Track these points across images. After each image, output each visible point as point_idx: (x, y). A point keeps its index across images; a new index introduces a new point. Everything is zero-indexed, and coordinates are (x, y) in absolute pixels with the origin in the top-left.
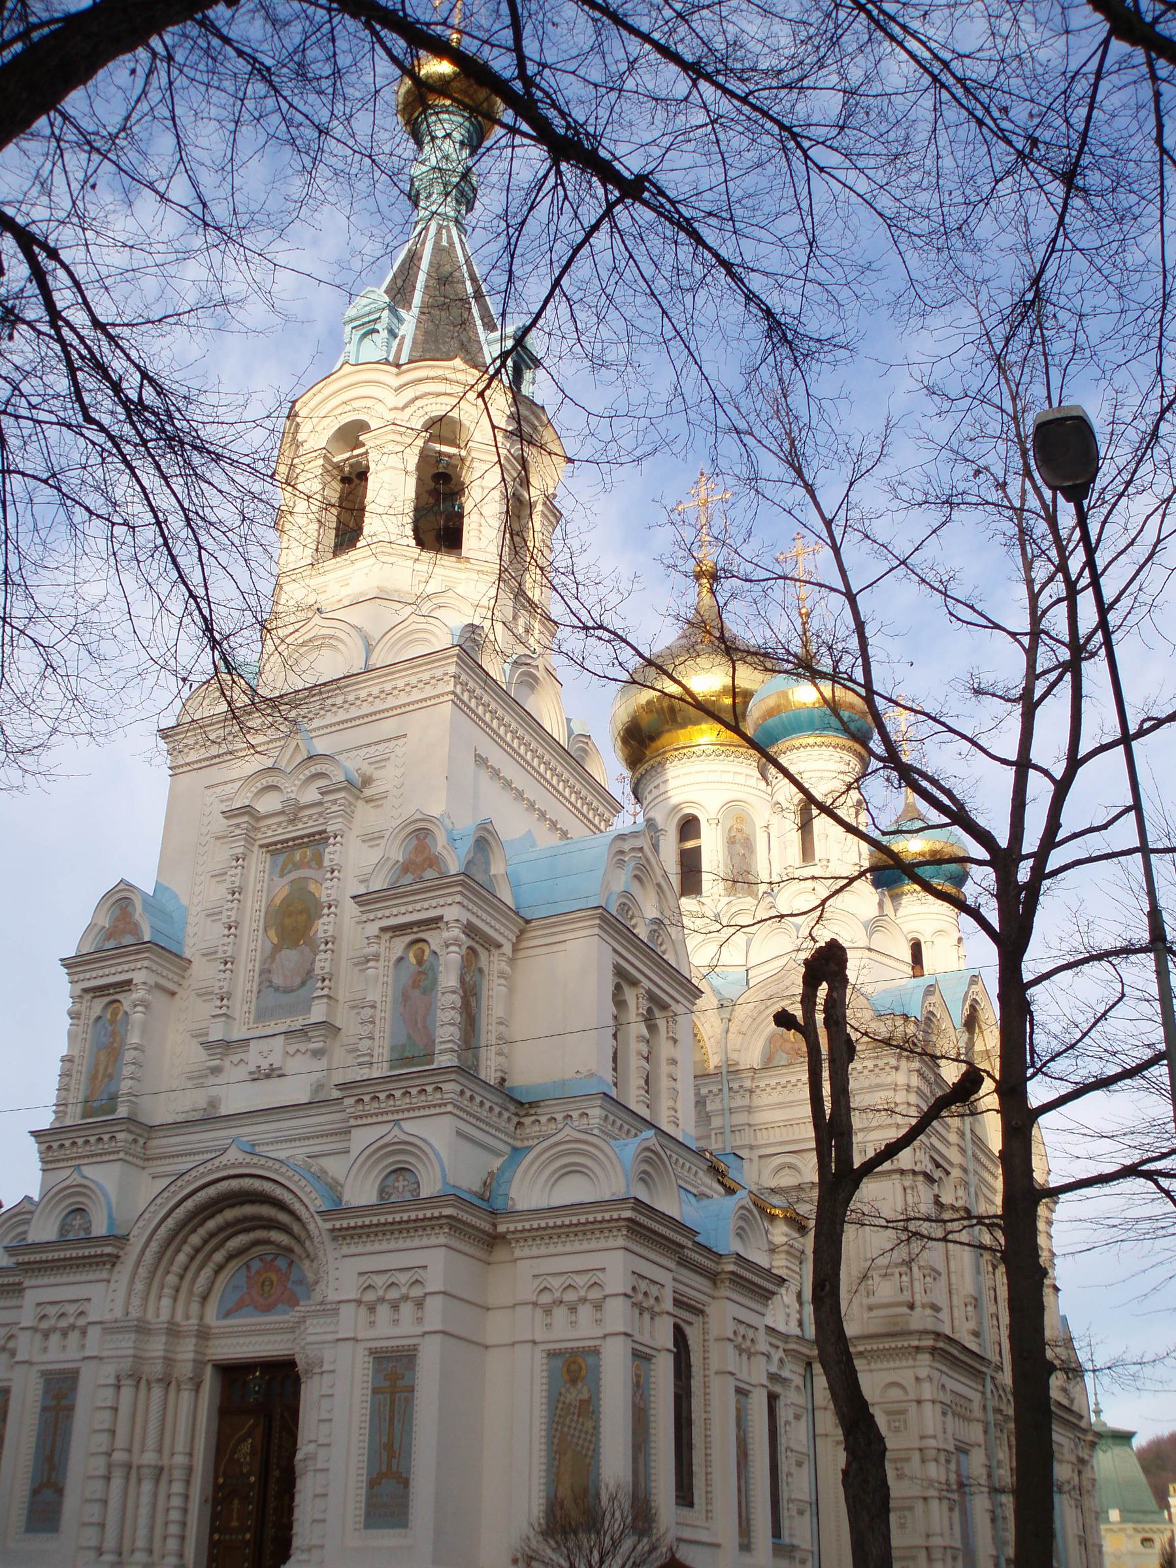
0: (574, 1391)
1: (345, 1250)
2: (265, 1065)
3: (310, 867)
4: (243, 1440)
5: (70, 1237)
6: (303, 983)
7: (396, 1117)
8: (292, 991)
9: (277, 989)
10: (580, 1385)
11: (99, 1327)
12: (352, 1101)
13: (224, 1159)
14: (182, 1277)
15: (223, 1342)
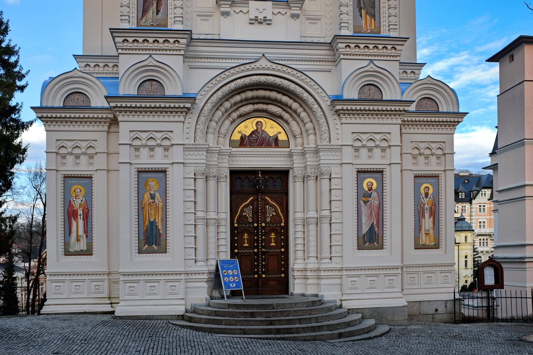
11: (182, 146)
15: (238, 159)
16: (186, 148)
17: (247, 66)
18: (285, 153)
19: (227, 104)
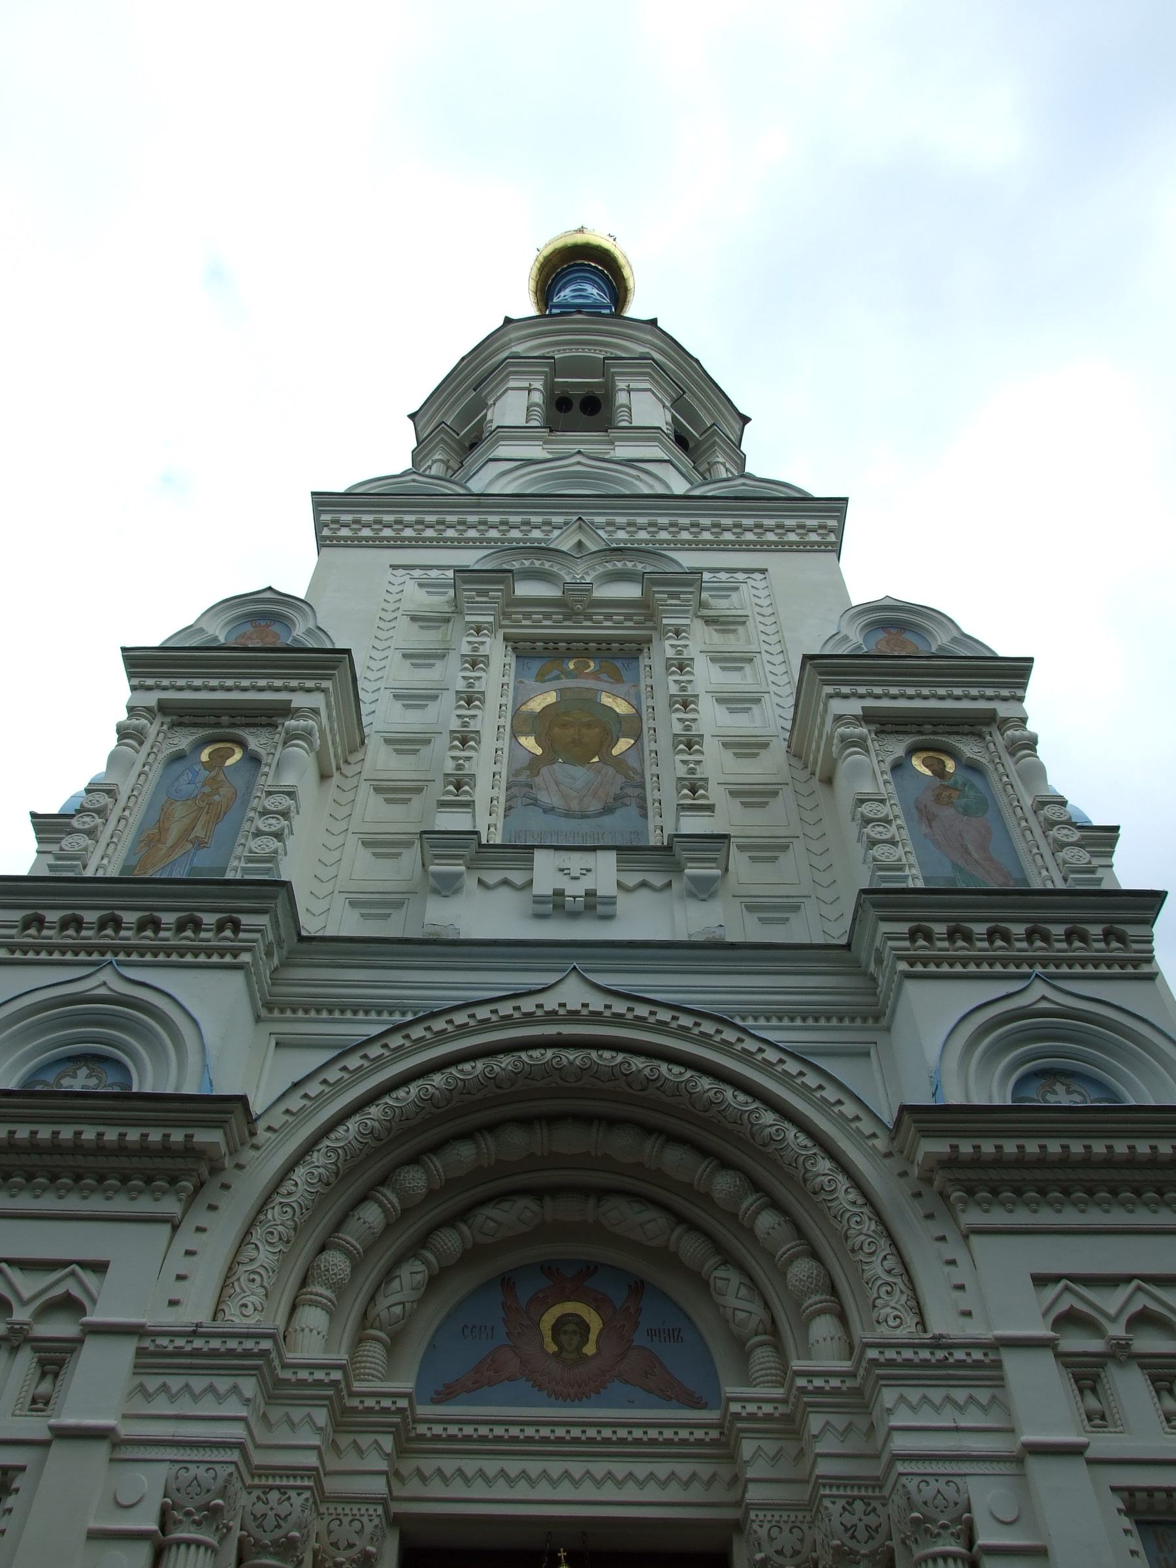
1: (973, 1217)
2: (575, 889)
3: (599, 679)
8: (584, 816)
11: (126, 1349)
12: (904, 928)
13: (550, 1002)
18: (699, 1434)
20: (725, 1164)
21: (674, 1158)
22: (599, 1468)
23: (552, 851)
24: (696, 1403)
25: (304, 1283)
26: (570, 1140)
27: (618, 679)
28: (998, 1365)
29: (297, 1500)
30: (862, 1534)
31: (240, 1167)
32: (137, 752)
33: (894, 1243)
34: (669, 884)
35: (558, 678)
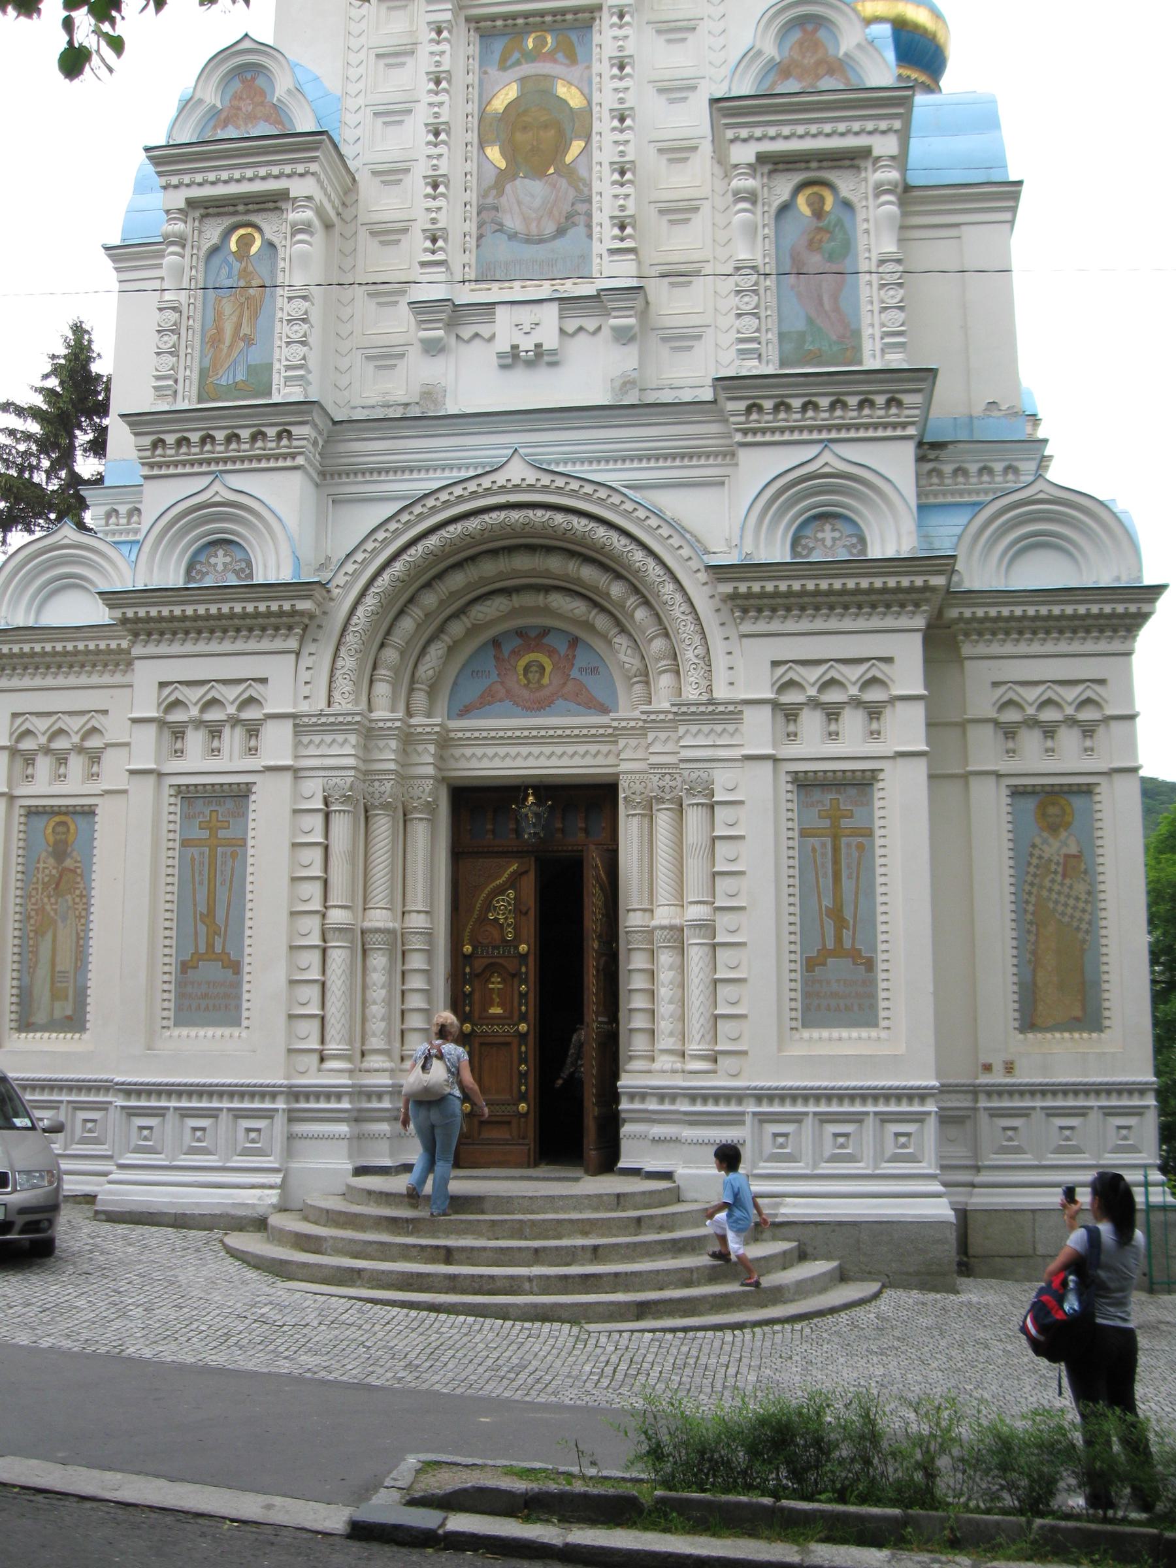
0: (1056, 844)
1: (747, 627)
2: (527, 344)
3: (555, 61)
4: (501, 890)
5: (208, 582)
6: (561, 232)
7: (824, 435)
8: (541, 241)
9: (513, 236)
10: (1064, 834)
11: (288, 725)
13: (500, 478)
14: (402, 654)
15: (468, 752)
16: (302, 726)
17: (472, 486)
19: (430, 600)
20: (619, 576)
21: (588, 573)
22: (548, 750)
23: (508, 307)
24: (604, 710)
25: (374, 668)
26: (523, 562)
27: (572, 59)
28: (741, 712)
29: (388, 785)
30: (667, 789)
31: (325, 613)
32: (183, 257)
33: (705, 638)
34: (600, 328)
35: (518, 63)
